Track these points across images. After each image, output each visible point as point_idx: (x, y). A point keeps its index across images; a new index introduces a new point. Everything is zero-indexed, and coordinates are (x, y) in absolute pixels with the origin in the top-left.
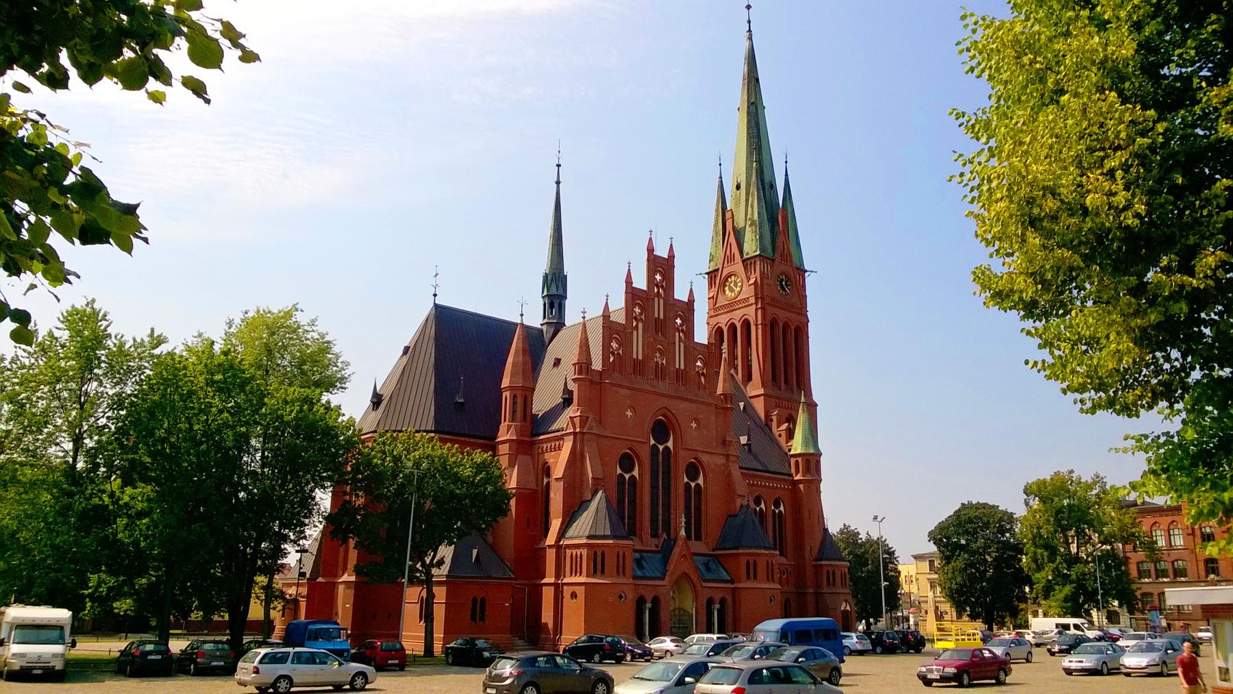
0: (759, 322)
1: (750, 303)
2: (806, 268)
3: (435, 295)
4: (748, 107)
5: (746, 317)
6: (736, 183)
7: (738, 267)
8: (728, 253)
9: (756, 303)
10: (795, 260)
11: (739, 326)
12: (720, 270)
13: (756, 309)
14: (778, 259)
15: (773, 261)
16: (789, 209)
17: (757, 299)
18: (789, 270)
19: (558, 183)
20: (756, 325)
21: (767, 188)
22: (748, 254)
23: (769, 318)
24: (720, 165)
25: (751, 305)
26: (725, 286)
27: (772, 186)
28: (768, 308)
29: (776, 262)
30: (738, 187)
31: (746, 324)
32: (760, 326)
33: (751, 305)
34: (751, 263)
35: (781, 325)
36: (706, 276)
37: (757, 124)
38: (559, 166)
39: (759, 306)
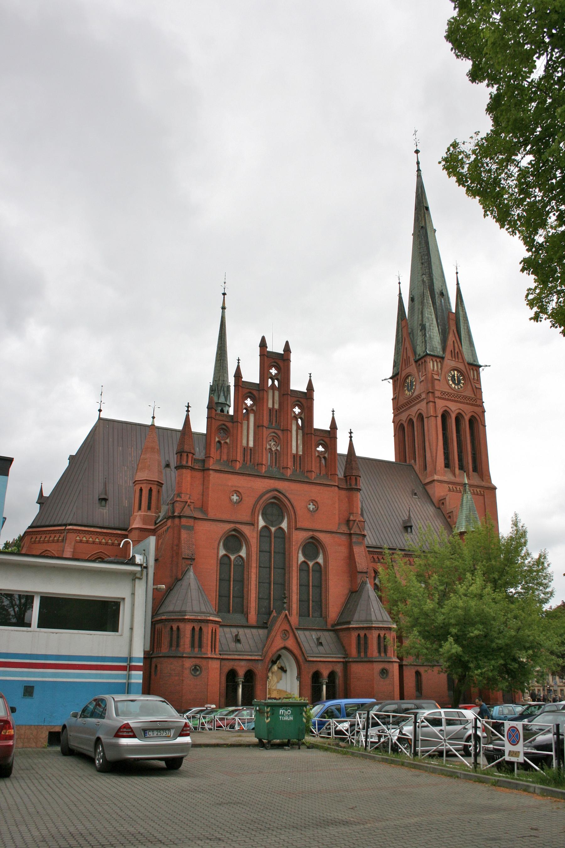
1: (422, 398)
2: (481, 362)
3: (100, 411)
4: (419, 231)
5: (420, 411)
8: (405, 357)
10: (468, 358)
13: (427, 403)
14: (448, 356)
15: (443, 358)
16: (461, 312)
18: (461, 366)
19: (223, 308)
21: (437, 296)
22: (419, 355)
27: (443, 294)
28: (437, 400)
29: (446, 359)
34: (422, 363)
35: (453, 416)
36: (391, 381)
37: (427, 243)
38: (224, 294)
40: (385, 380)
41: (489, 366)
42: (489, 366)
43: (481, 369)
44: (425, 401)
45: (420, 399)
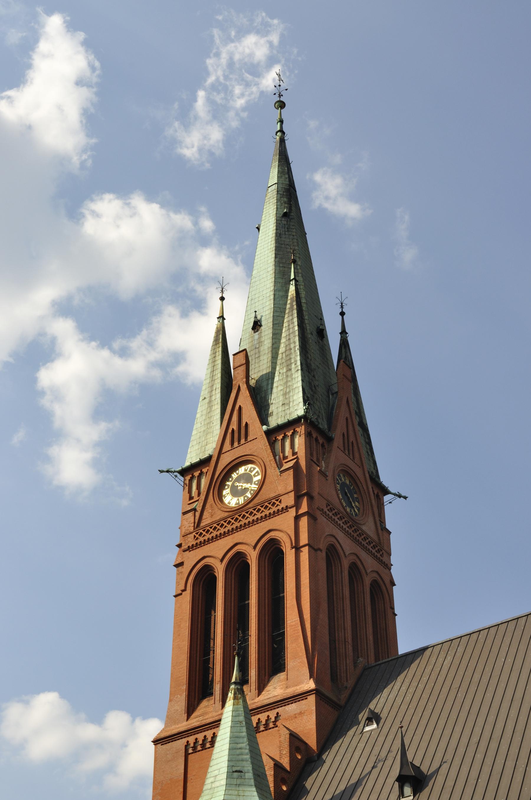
0: (304, 539)
1: (283, 505)
5: (272, 534)
6: (252, 320)
8: (234, 425)
9: (297, 505)
12: (214, 459)
13: (297, 518)
17: (298, 498)
20: (297, 548)
23: (323, 545)
25: (287, 508)
26: (222, 486)
30: (257, 325)
32: (305, 551)
33: (287, 508)
39: (304, 508)
40: (168, 471)
41: (405, 498)
42: (405, 498)
43: (387, 498)
44: (292, 512)
45: (275, 509)
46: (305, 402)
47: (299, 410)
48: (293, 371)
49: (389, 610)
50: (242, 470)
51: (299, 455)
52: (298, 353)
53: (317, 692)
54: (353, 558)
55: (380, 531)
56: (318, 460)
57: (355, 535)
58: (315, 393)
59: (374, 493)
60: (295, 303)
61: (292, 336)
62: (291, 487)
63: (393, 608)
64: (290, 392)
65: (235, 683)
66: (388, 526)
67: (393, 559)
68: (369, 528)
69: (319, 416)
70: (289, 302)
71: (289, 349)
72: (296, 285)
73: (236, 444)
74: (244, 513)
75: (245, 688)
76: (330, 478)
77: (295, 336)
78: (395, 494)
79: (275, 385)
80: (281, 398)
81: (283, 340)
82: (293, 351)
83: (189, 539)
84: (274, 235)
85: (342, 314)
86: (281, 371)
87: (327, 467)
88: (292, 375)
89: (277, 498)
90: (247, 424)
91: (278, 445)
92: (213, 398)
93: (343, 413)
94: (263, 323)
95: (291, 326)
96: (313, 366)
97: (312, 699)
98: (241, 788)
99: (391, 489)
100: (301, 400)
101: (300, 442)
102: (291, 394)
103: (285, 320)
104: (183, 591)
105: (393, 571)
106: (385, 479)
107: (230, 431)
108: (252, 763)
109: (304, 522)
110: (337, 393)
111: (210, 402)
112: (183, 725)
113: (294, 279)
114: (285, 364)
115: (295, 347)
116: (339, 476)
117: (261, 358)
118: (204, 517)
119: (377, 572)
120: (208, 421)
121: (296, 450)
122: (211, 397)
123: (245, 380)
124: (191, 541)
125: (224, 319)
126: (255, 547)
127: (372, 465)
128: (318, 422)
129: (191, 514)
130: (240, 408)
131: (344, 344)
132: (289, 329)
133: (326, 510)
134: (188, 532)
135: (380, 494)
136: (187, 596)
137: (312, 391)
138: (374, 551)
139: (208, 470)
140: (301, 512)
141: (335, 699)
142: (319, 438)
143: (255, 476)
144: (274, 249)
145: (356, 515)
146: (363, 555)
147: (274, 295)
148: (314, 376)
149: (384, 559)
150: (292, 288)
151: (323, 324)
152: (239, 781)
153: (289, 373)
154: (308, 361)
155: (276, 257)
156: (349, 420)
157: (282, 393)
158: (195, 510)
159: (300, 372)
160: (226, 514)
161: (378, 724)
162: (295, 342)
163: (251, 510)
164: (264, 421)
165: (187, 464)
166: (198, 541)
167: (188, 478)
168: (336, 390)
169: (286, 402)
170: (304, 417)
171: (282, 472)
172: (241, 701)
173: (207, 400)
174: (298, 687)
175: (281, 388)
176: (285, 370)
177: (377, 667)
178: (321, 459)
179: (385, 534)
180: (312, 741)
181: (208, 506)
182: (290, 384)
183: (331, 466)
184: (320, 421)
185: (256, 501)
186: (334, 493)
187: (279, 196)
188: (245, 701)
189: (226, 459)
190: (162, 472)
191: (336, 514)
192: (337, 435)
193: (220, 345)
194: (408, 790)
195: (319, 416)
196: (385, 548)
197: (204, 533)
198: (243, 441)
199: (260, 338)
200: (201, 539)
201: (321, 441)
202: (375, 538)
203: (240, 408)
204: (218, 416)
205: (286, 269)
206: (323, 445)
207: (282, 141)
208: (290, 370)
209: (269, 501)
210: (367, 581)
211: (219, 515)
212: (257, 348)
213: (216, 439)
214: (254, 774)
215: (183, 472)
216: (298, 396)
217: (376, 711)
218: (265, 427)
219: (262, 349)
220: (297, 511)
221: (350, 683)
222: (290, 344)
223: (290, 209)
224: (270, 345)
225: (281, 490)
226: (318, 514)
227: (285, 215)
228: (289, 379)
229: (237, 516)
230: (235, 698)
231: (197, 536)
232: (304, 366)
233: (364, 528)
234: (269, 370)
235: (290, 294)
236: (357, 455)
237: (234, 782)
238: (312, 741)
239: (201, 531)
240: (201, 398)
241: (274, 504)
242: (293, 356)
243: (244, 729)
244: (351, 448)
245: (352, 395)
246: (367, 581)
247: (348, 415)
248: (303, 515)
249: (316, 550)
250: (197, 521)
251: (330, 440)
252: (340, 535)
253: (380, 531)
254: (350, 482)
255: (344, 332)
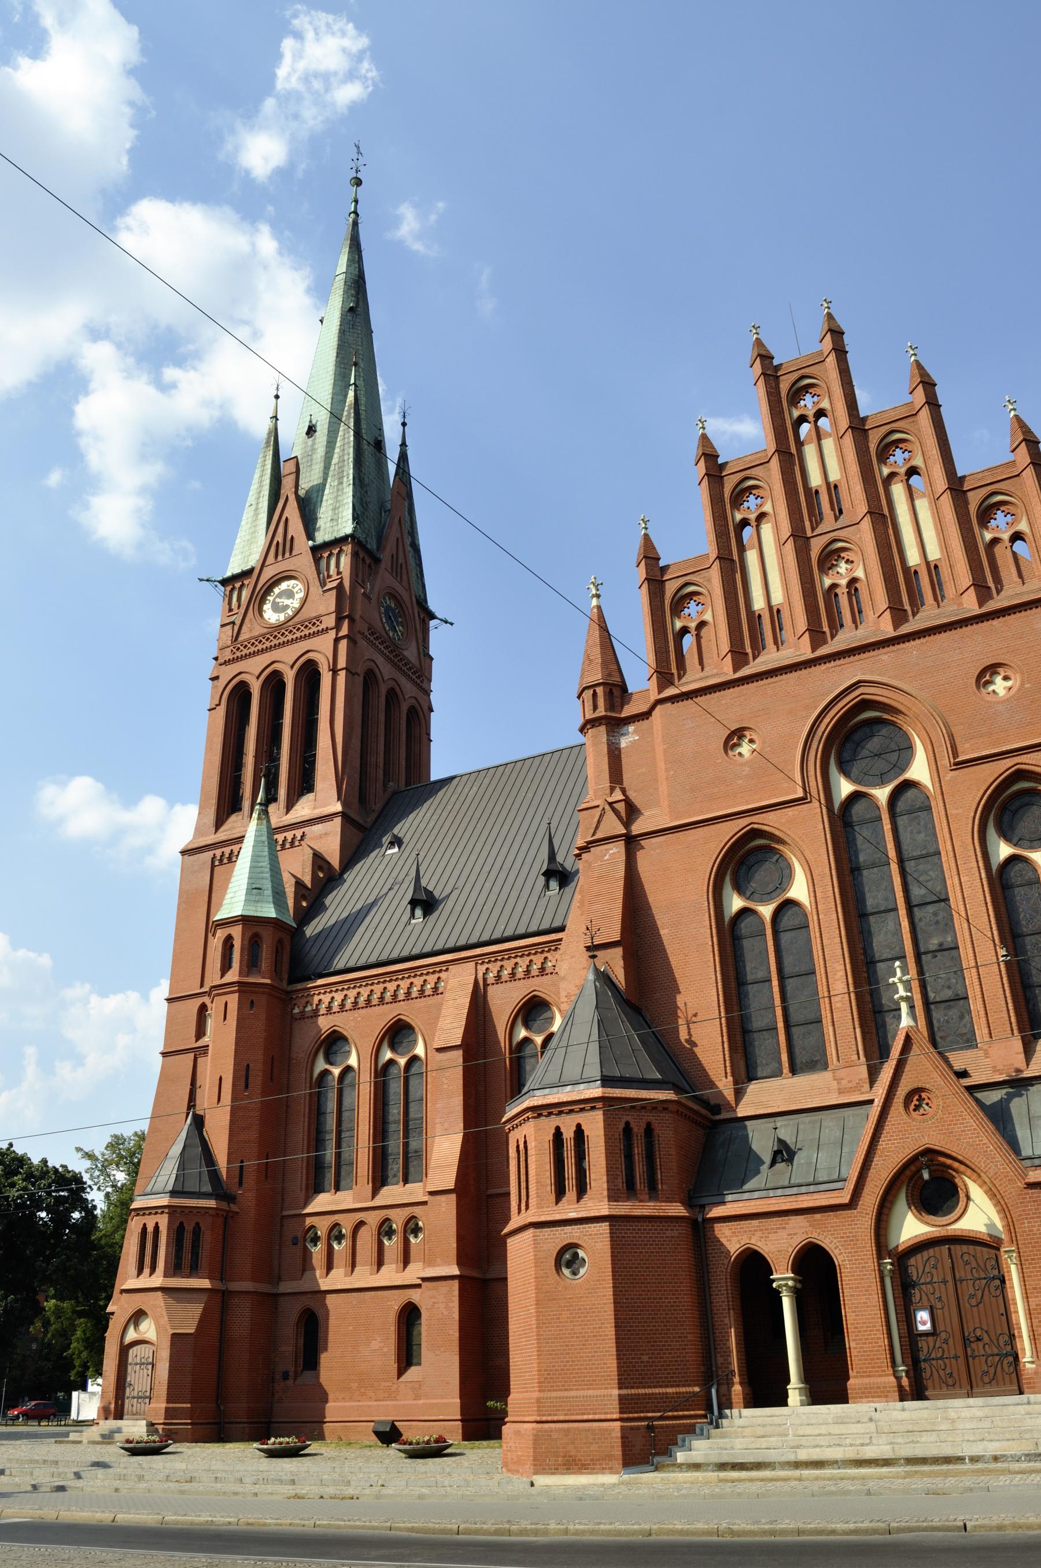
0: (342, 663)
1: (323, 626)
5: (310, 655)
6: (307, 424)
7: (302, 560)
8: (279, 538)
9: (338, 627)
11: (290, 677)
12: (256, 572)
13: (337, 640)
17: (339, 621)
20: (335, 671)
23: (361, 670)
24: (277, 397)
25: (327, 630)
26: (263, 601)
30: (311, 430)
31: (309, 674)
32: (342, 674)
33: (327, 630)
39: (344, 631)
41: (452, 624)
42: (452, 624)
43: (433, 623)
44: (332, 634)
45: (315, 629)
46: (354, 519)
47: (347, 527)
48: (345, 485)
49: (424, 737)
50: (284, 585)
51: (343, 574)
52: (352, 466)
53: (344, 815)
54: (392, 683)
55: (422, 656)
56: (363, 581)
57: (396, 660)
58: (366, 510)
59: (420, 618)
60: (352, 411)
61: (346, 446)
62: (333, 608)
63: (429, 734)
64: (339, 507)
65: (260, 804)
66: (431, 653)
67: (434, 686)
68: (411, 653)
69: (368, 535)
70: (346, 408)
71: (342, 461)
72: (355, 391)
73: (280, 558)
74: (283, 631)
75: (272, 808)
76: (374, 601)
77: (349, 447)
78: (441, 620)
79: (325, 498)
80: (330, 513)
81: (337, 450)
82: (346, 463)
83: (226, 653)
84: (337, 331)
85: (404, 424)
86: (332, 484)
87: (372, 589)
88: (343, 489)
89: (318, 618)
90: (292, 537)
91: (323, 563)
92: (260, 505)
93: (393, 533)
94: (318, 429)
95: (346, 436)
96: (367, 481)
97: (338, 821)
98: (259, 905)
99: (437, 614)
100: (351, 517)
101: (345, 561)
102: (341, 509)
103: (341, 429)
104: (217, 705)
105: (432, 696)
106: (433, 605)
107: (275, 543)
108: (272, 881)
109: (343, 645)
110: (389, 510)
111: (256, 509)
112: (211, 838)
113: (354, 384)
114: (336, 477)
115: (348, 459)
116: (384, 598)
117: (313, 467)
118: (243, 631)
119: (416, 699)
120: (253, 529)
121: (341, 570)
122: (257, 504)
123: (294, 490)
124: (228, 655)
125: (277, 419)
126: (292, 667)
127: (421, 589)
128: (367, 542)
129: (229, 627)
130: (287, 519)
131: (403, 458)
132: (344, 439)
133: (367, 634)
134: (225, 645)
135: (426, 619)
136: (222, 711)
137: (363, 507)
138: (414, 677)
139: (250, 582)
140: (341, 634)
141: (361, 822)
142: (366, 558)
143: (297, 593)
144: (336, 347)
145: (399, 639)
146: (403, 680)
147: (332, 398)
148: (366, 492)
149: (424, 685)
150: (351, 394)
151: (382, 435)
152: (257, 898)
153: (340, 487)
154: (362, 475)
155: (337, 357)
156: (400, 540)
157: (331, 507)
158: (233, 623)
159: (351, 486)
160: (266, 630)
161: (399, 848)
162: (349, 454)
163: (291, 628)
164: (310, 536)
165: (228, 574)
166: (235, 656)
167: (229, 588)
168: (389, 507)
169: (335, 517)
170: (352, 536)
171: (324, 592)
172: (265, 821)
173: (253, 507)
174: (325, 809)
175: (330, 502)
176: (336, 483)
177: (406, 792)
178: (366, 580)
179: (428, 660)
180: (335, 861)
181: (247, 620)
182: (340, 498)
183: (376, 589)
184: (368, 540)
185: (296, 619)
186: (377, 616)
187: (346, 287)
188: (269, 821)
189: (268, 573)
190: (201, 580)
191: (377, 638)
192: (385, 557)
193: (272, 448)
194: (419, 912)
195: (368, 535)
196: (426, 674)
197: (242, 648)
198: (287, 555)
199: (313, 444)
200: (238, 654)
201: (368, 561)
202: (417, 664)
203: (287, 519)
204: (264, 525)
205: (347, 371)
206: (370, 566)
207: (355, 224)
208: (342, 483)
209: (310, 621)
210: (405, 708)
211: (258, 631)
212: (310, 454)
213: (260, 549)
214: (273, 892)
215: (224, 582)
216: (347, 513)
217: (399, 835)
218: (311, 543)
219: (314, 457)
220: (337, 634)
221: (378, 807)
222: (343, 455)
223: (357, 303)
224: (323, 454)
225: (322, 610)
226: (359, 637)
227: (351, 309)
228: (340, 493)
229: (276, 633)
230: (259, 818)
231: (234, 650)
232: (357, 480)
233: (406, 653)
234: (320, 481)
235: (348, 400)
236: (405, 577)
237: (253, 898)
238: (335, 861)
239: (239, 646)
240: (248, 504)
241: (314, 624)
242: (345, 469)
243: (266, 849)
244: (399, 570)
245: (407, 514)
246: (405, 708)
247: (399, 535)
248: (343, 637)
249: (353, 674)
250: (235, 635)
251: (377, 561)
252: (380, 660)
253: (422, 656)
254: (395, 605)
255: (403, 444)
